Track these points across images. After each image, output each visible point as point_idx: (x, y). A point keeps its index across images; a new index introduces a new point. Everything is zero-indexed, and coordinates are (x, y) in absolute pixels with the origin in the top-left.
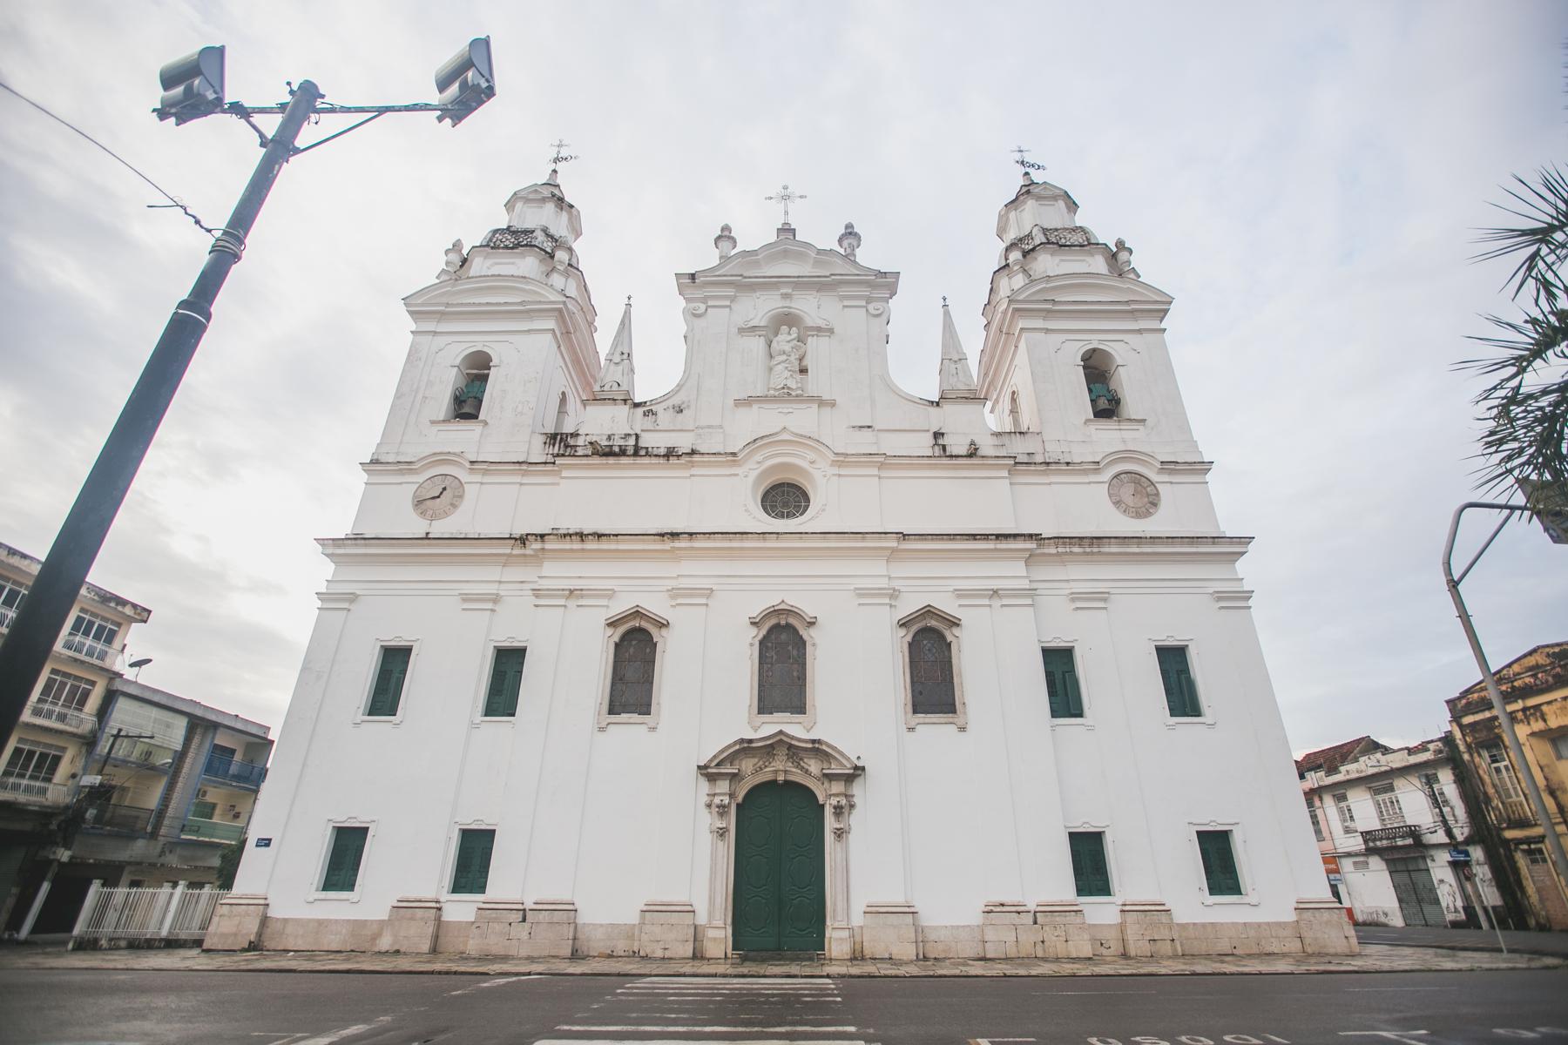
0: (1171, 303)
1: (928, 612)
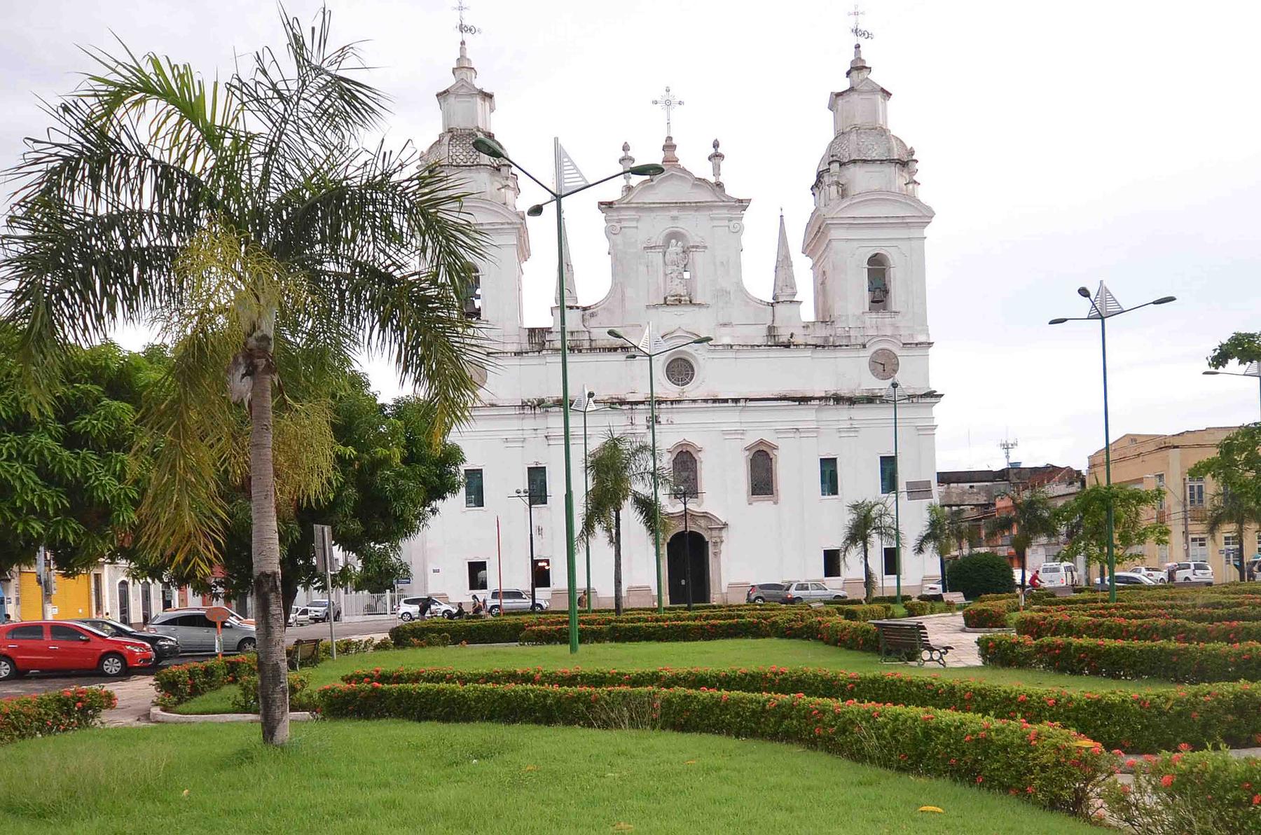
0: (932, 217)
1: (762, 442)
